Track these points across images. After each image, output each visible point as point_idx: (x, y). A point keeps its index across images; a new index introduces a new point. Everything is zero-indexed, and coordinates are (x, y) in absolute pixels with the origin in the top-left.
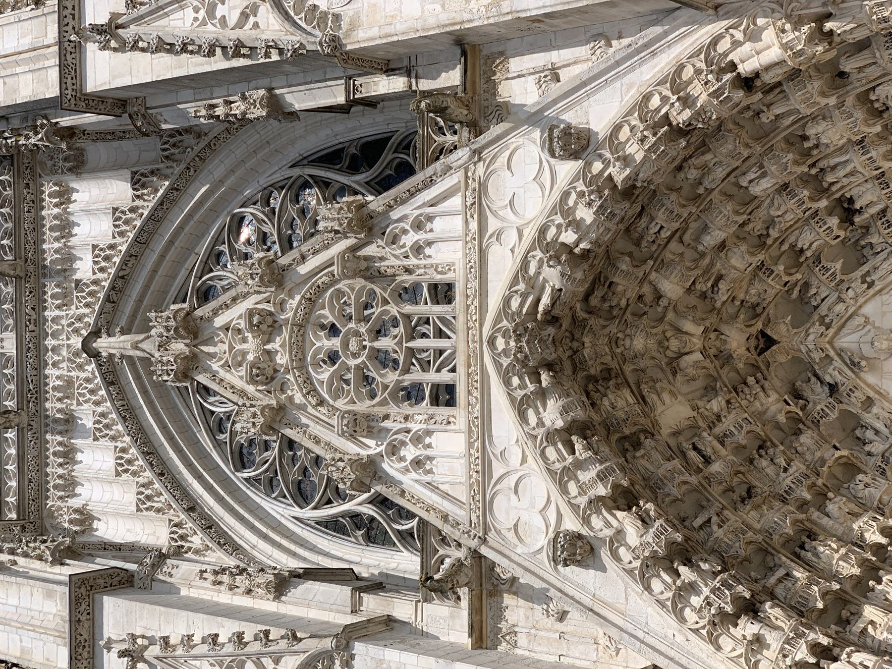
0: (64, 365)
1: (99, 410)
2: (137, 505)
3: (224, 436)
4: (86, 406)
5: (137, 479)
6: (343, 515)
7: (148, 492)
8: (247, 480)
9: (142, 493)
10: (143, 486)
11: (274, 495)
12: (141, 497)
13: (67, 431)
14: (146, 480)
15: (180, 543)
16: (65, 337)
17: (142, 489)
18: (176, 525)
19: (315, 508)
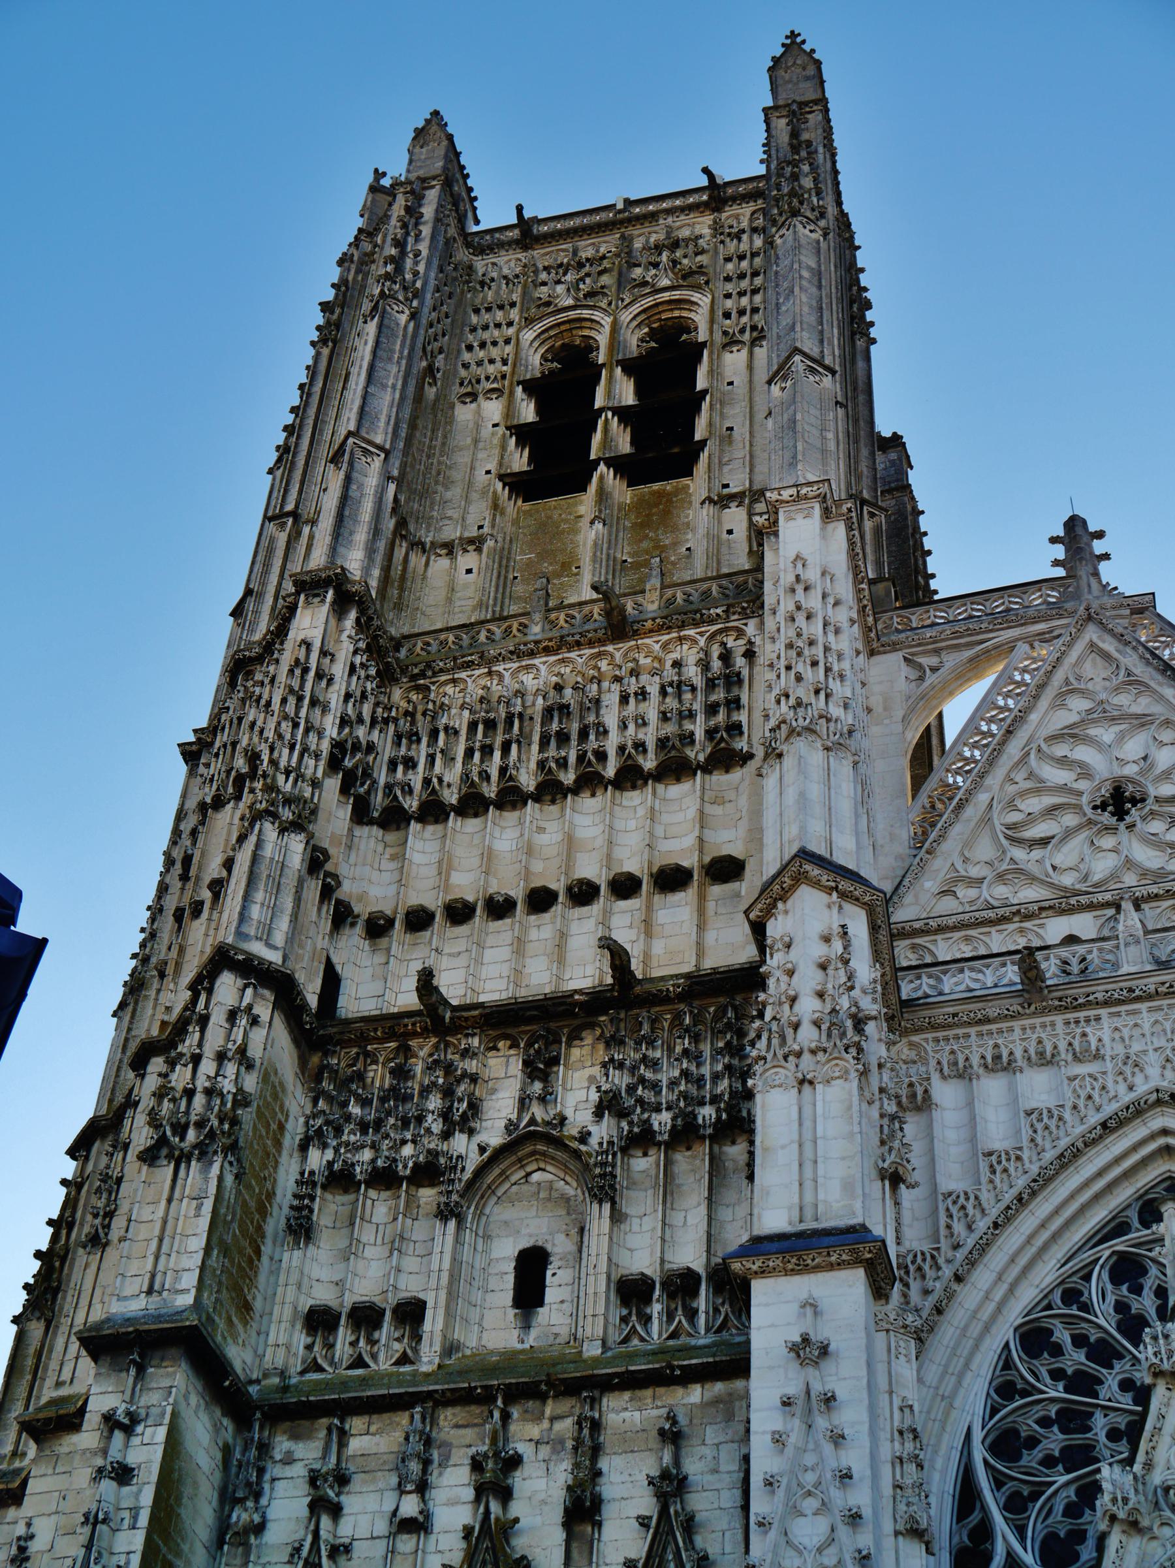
0: (1120, 1049)
1: (1067, 1115)
2: (950, 1194)
3: (1059, 1302)
4: (1069, 1094)
5: (985, 1186)
6: (984, 1509)
7: (970, 1210)
8: (1007, 1344)
9: (967, 1199)
10: (976, 1198)
11: (992, 1393)
12: (962, 1200)
13: (1029, 1059)
14: (985, 1204)
15: (912, 1268)
16: (1157, 1045)
17: (972, 1197)
18: (933, 1257)
19: (985, 1461)
